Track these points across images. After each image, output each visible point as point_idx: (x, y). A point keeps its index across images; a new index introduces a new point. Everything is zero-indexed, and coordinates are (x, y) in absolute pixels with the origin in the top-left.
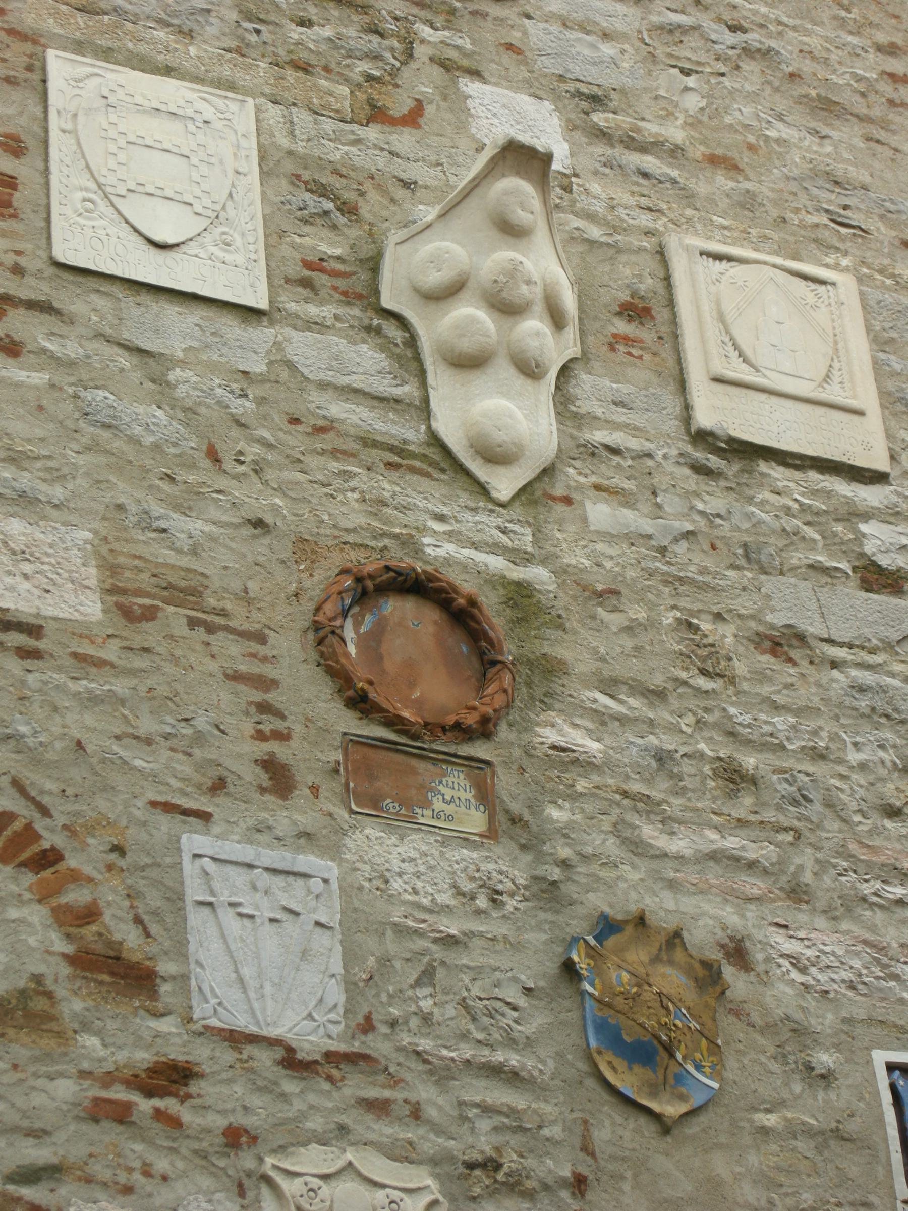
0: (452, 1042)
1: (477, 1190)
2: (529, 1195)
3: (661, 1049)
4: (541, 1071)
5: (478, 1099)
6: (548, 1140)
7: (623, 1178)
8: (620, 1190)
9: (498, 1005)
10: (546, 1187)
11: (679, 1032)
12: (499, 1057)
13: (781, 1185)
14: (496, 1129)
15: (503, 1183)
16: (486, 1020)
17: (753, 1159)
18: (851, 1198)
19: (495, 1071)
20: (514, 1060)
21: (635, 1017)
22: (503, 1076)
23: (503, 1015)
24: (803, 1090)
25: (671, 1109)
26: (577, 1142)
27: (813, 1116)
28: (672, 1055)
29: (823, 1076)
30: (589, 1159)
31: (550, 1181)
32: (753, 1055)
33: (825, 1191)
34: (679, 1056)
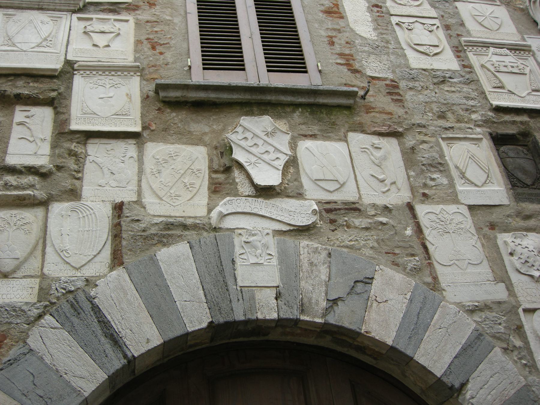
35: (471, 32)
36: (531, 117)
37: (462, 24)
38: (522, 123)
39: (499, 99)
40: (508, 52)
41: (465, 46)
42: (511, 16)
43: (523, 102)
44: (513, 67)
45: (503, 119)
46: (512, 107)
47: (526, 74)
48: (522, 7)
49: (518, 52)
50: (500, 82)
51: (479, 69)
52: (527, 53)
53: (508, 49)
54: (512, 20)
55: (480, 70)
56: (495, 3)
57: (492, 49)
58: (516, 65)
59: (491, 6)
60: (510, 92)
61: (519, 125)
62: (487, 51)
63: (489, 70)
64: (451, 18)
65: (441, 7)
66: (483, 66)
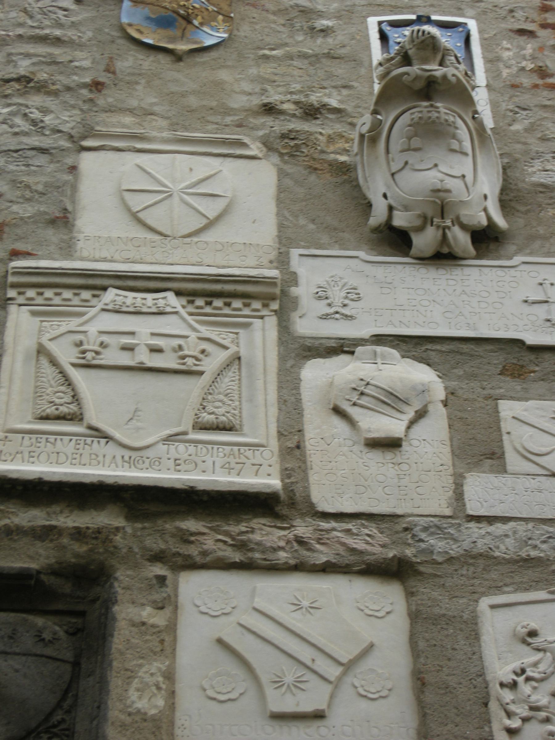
0: (11, 28)
1: (9, 92)
2: (55, 94)
3: (180, 20)
4: (79, 37)
5: (22, 51)
6: (76, 67)
7: (137, 83)
8: (134, 89)
9: (51, 9)
10: (69, 89)
11: (196, 11)
12: (47, 31)
13: (275, 81)
14: (34, 64)
15: (32, 87)
16: (40, 16)
17: (253, 71)
18: (333, 84)
19: (43, 39)
20: (58, 32)
21: (159, 4)
22: (48, 41)
23: (55, 13)
24: (305, 39)
25: (182, 47)
26: (102, 67)
27: (310, 49)
28: (189, 22)
29: (322, 31)
30: (110, 75)
31: (72, 85)
32: (264, 24)
33: (313, 82)
34: (196, 23)
35: (80, 244)
36: (133, 515)
37: (63, 220)
38: (79, 534)
39: (32, 456)
40: (172, 301)
41: (14, 286)
42: (281, 189)
43: (131, 463)
44: (156, 350)
45: (6, 521)
46: (56, 479)
47: (201, 373)
48: (343, 158)
49: (218, 303)
50: (76, 398)
51: (20, 357)
52: (256, 305)
53: (179, 293)
54: (279, 201)
55: (19, 366)
56: (239, 152)
57: (111, 296)
58: (176, 342)
59: (220, 160)
60: (97, 433)
61: (65, 541)
62: (94, 301)
63: (54, 362)
64: (29, 200)
65: (12, 167)
66: (41, 351)
